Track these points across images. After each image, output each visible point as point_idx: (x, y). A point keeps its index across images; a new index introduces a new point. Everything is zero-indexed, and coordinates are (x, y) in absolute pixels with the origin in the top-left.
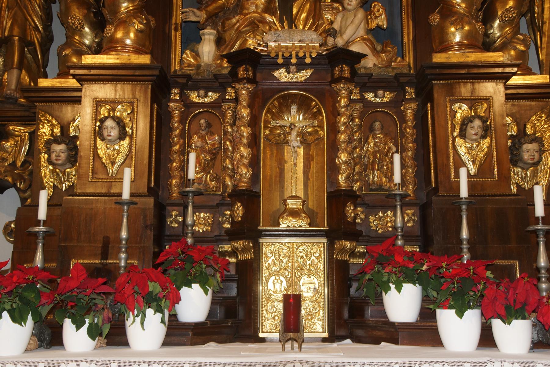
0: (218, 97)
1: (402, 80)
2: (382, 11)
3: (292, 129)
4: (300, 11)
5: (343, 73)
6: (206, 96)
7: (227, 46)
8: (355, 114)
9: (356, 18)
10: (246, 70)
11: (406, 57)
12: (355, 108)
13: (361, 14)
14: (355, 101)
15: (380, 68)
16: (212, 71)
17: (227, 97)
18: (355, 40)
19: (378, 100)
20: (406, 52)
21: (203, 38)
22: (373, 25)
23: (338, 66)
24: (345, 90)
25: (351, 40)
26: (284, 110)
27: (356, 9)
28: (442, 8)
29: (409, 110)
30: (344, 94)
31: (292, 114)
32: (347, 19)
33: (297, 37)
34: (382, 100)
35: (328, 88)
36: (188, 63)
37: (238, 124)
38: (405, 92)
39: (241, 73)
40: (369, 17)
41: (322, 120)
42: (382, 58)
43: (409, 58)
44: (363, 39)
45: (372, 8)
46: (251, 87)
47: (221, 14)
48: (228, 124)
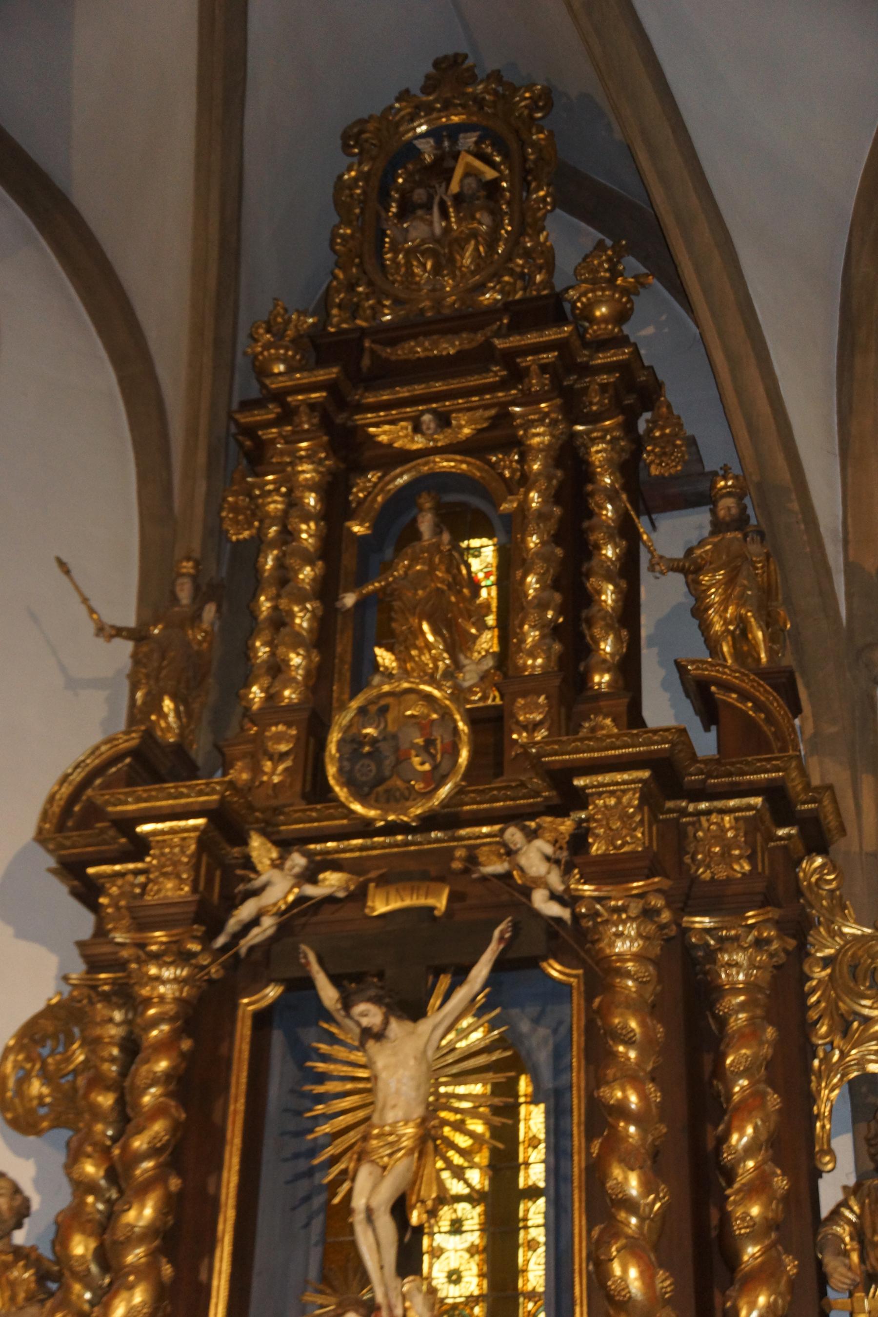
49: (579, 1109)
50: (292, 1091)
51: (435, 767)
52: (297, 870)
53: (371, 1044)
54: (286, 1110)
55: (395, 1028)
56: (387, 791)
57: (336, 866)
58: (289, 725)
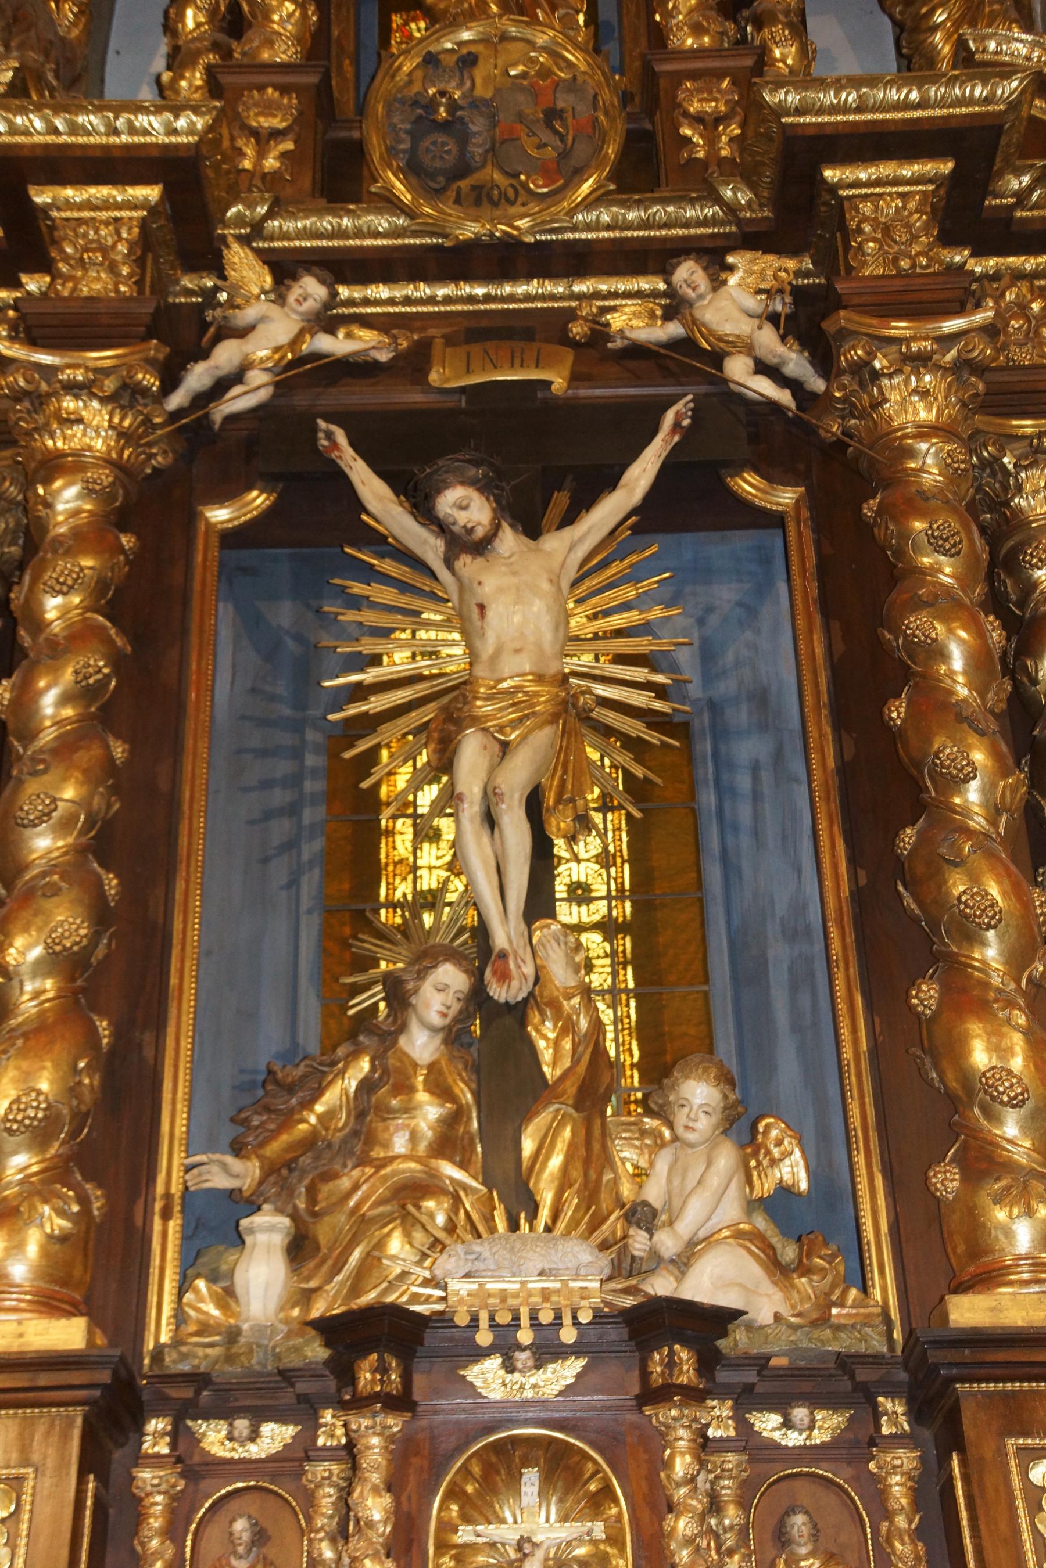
0: (293, 1437)
1: (863, 1375)
2: (790, 1143)
3: (525, 1555)
4: (542, 1151)
5: (676, 1371)
6: (254, 1436)
7: (323, 1262)
8: (723, 1488)
9: (713, 1169)
10: (382, 1369)
11: (873, 1286)
12: (723, 1470)
13: (726, 1157)
14: (722, 1445)
15: (795, 1328)
16: (274, 1348)
17: (320, 1442)
18: (712, 1235)
19: (793, 1439)
20: (872, 1271)
21: (248, 1240)
22: (765, 1187)
23: (658, 1348)
24: (683, 1426)
25: (702, 1234)
26: (500, 1484)
27: (712, 1144)
28: (965, 1148)
29: (896, 1474)
30: (681, 1439)
31: (525, 1500)
32: (685, 1171)
33: (535, 1261)
34: (809, 1437)
35: (632, 1417)
36: (199, 1322)
37: (356, 1550)
38: (876, 1415)
39: (366, 1377)
40: (753, 1163)
41: (619, 1517)
42: (798, 1292)
43: (884, 1290)
44: (738, 1235)
45: (760, 1138)
46: (394, 1423)
47: (305, 1160)
48: (322, 1534)
49: (816, 685)
50: (253, 690)
51: (564, 155)
52: (309, 305)
53: (466, 563)
54: (243, 717)
55: (509, 540)
56: (477, 189)
57: (365, 322)
58: (284, 90)
